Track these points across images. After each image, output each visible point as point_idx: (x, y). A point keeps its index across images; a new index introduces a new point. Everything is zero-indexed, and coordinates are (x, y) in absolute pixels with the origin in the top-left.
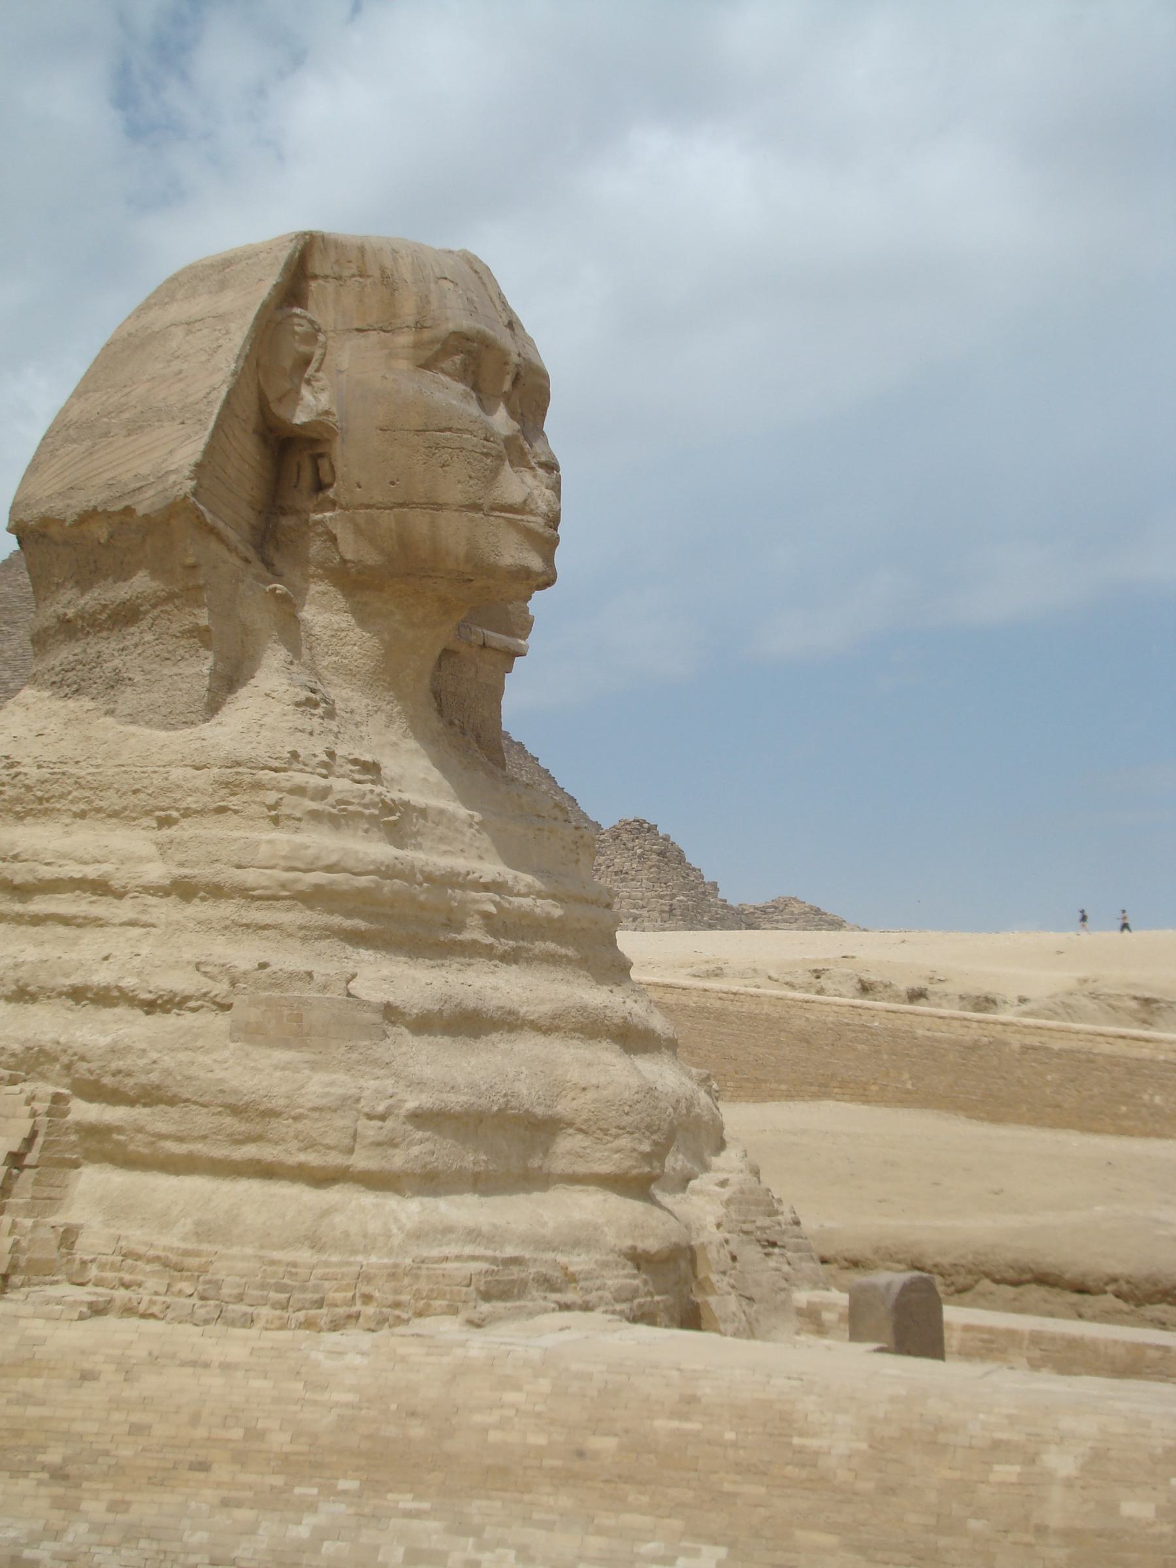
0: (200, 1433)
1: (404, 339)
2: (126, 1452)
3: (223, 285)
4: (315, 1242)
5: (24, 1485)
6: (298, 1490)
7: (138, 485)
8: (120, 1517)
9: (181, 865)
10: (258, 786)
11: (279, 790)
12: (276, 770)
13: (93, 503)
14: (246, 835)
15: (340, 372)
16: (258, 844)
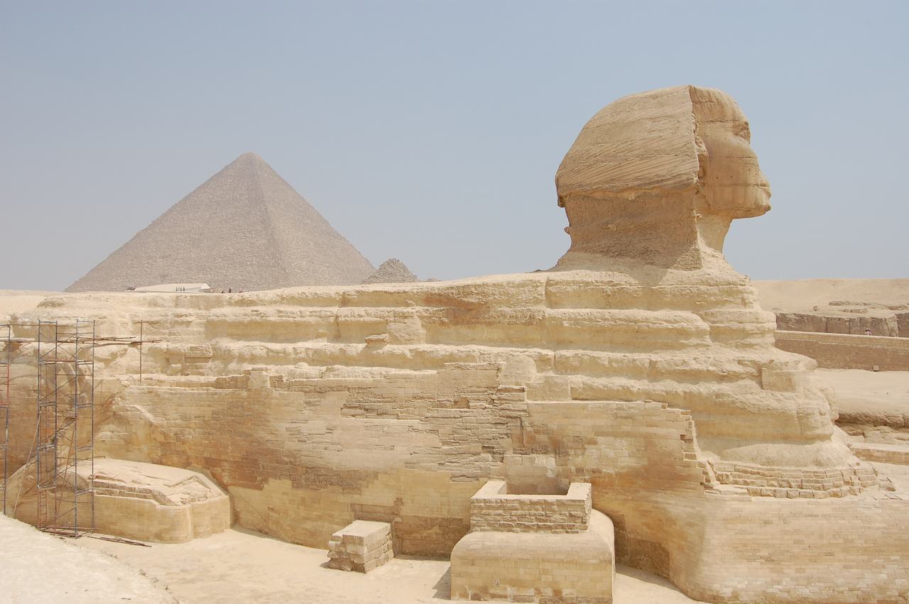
0: (825, 541)
1: (730, 124)
2: (796, 550)
3: (661, 105)
4: (819, 464)
5: (756, 564)
6: (875, 561)
7: (660, 179)
8: (802, 575)
9: (714, 322)
10: (741, 292)
11: (747, 293)
12: (742, 285)
13: (631, 185)
14: (739, 310)
15: (707, 136)
16: (746, 313)
